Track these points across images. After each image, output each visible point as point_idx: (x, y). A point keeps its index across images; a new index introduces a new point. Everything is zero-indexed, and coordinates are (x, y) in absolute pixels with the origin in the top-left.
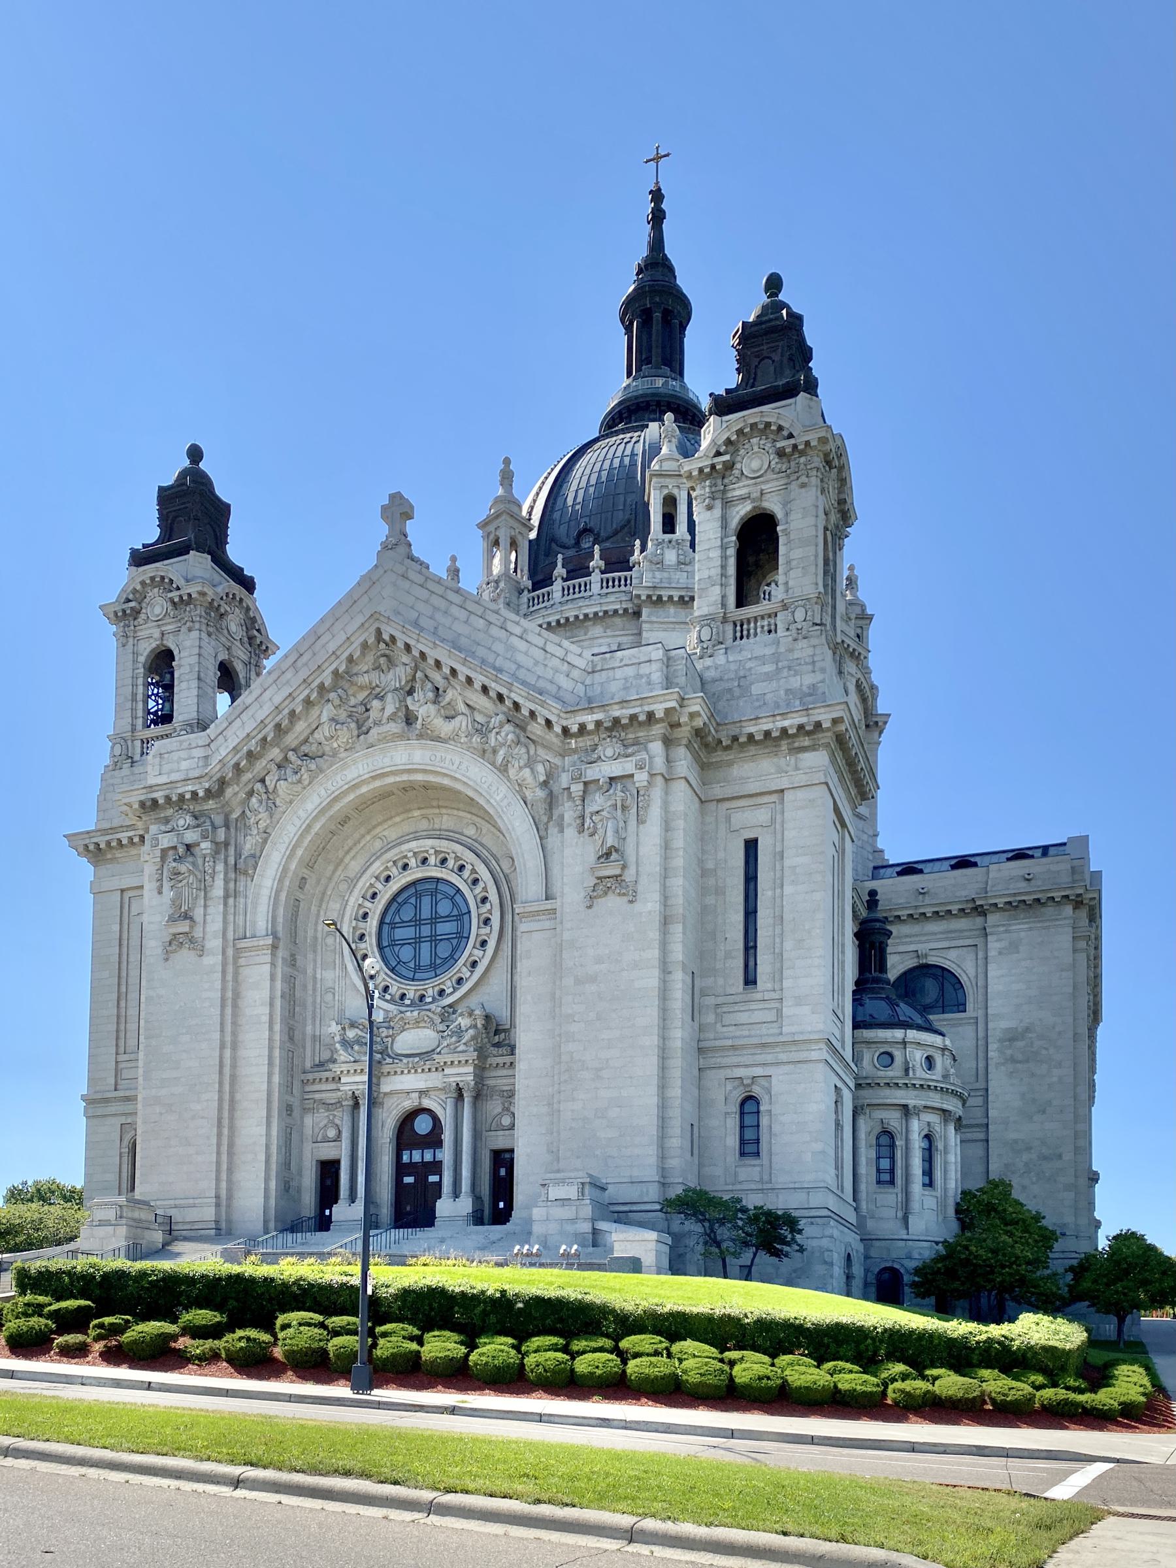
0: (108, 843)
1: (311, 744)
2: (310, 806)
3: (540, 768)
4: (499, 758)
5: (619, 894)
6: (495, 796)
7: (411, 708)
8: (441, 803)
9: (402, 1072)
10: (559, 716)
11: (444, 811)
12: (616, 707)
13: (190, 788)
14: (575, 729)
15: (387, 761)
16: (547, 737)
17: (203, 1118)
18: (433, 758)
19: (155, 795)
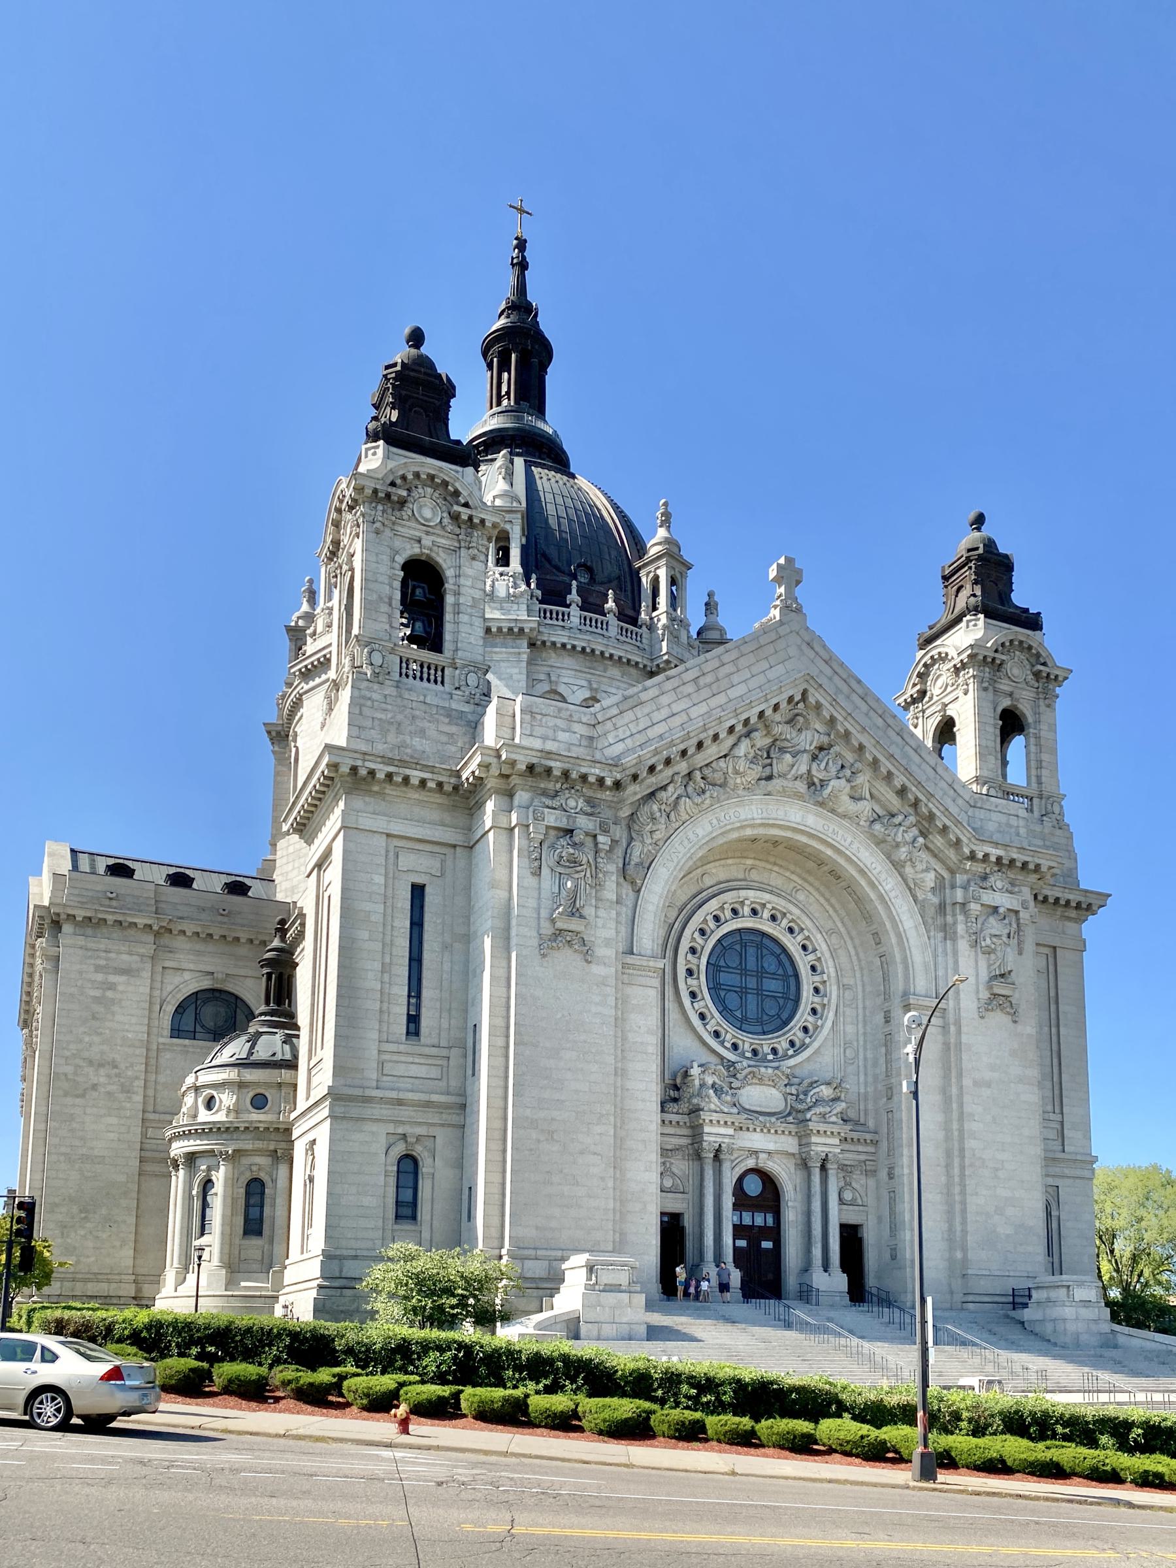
0: (389, 776)
1: (714, 771)
2: (701, 832)
3: (932, 875)
4: (903, 853)
5: (1008, 1013)
6: (884, 884)
7: (814, 772)
8: (778, 862)
9: (755, 1130)
10: (969, 839)
11: (776, 868)
12: (1015, 850)
13: (597, 771)
14: (980, 855)
15: (781, 814)
16: (947, 852)
17: (595, 1153)
18: (826, 828)
19: (552, 764)
